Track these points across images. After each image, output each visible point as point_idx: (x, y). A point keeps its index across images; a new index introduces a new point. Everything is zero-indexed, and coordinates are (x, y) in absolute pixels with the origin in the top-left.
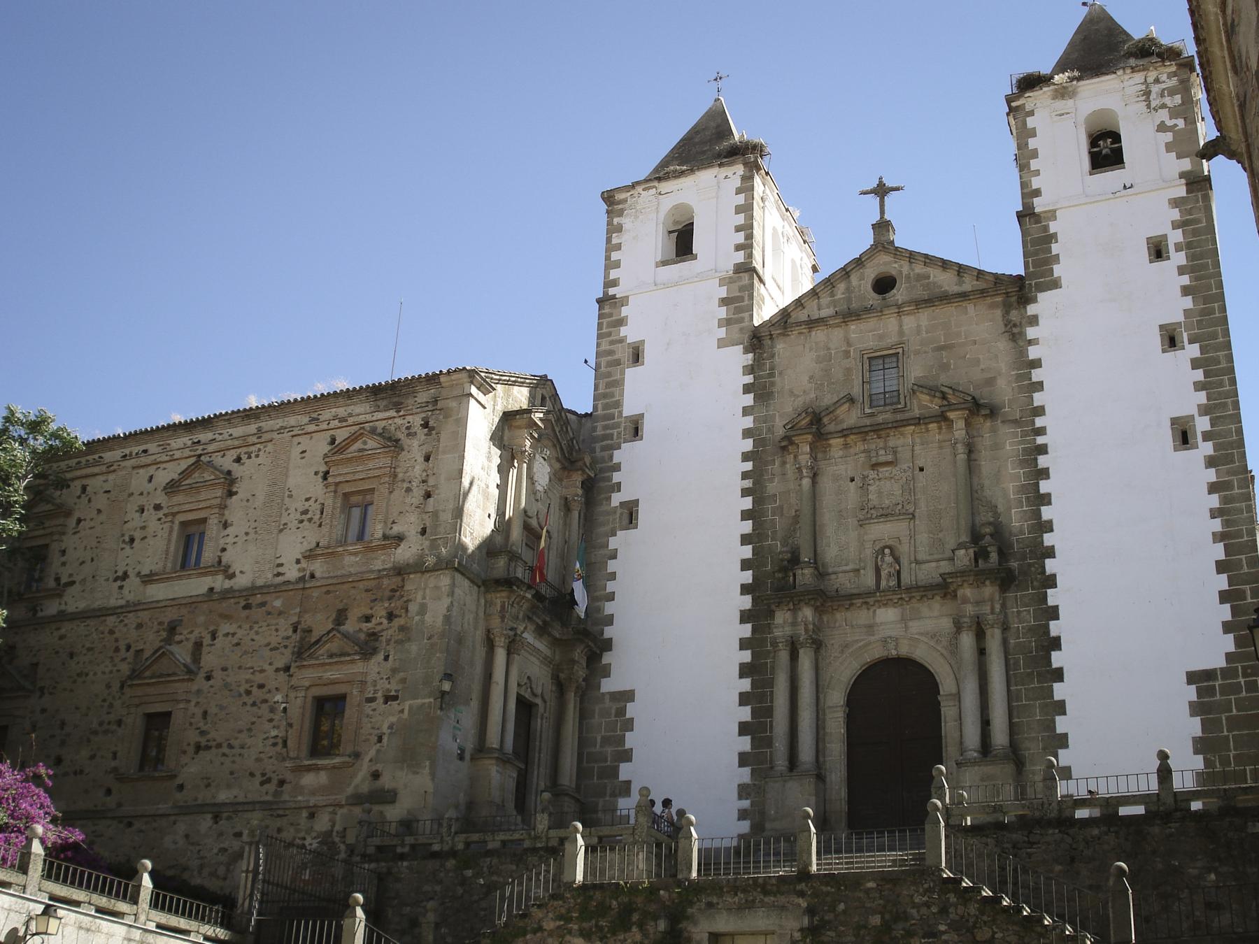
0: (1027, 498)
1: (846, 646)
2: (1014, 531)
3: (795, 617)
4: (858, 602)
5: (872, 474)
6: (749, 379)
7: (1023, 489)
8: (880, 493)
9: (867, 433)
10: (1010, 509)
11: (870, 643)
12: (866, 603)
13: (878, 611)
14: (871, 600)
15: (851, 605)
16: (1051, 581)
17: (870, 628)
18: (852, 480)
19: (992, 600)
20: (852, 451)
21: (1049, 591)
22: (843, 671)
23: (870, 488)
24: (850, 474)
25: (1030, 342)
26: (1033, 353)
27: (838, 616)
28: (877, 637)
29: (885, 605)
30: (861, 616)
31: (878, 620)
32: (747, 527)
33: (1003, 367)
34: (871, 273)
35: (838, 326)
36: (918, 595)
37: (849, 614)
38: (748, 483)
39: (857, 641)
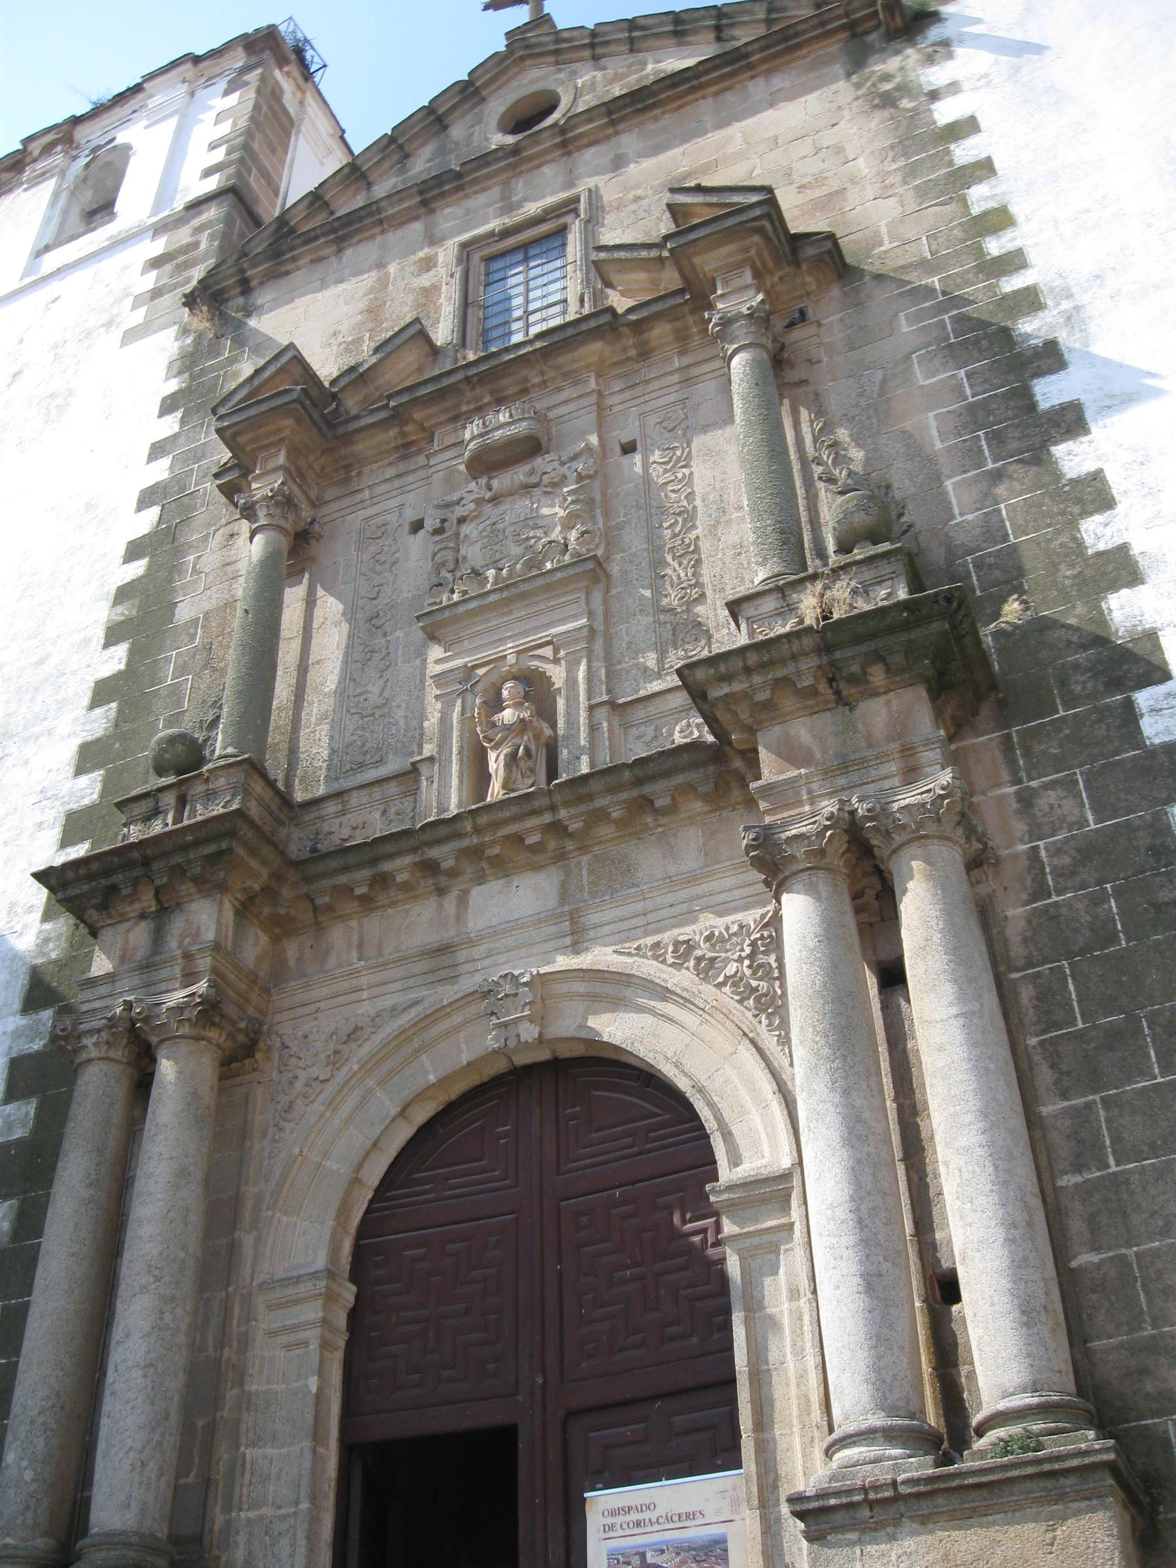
0: (997, 439)
1: (354, 1035)
2: (961, 538)
3: (158, 937)
4: (401, 867)
5: (475, 489)
6: (173, 386)
7: (974, 416)
8: (494, 534)
9: (453, 389)
10: (937, 479)
11: (440, 1012)
12: (431, 868)
13: (477, 894)
14: (444, 854)
15: (383, 881)
16: (1139, 663)
17: (442, 957)
18: (417, 526)
19: (900, 730)
20: (421, 460)
21: (1143, 698)
22: (337, 1139)
23: (466, 529)
24: (410, 515)
25: (934, 95)
26: (945, 113)
27: (338, 936)
28: (468, 983)
29: (501, 867)
30: (419, 922)
31: (476, 922)
32: (99, 722)
33: (863, 166)
34: (497, 106)
35: (410, 217)
36: (614, 805)
37: (373, 925)
38: (123, 611)
39: (394, 1011)
